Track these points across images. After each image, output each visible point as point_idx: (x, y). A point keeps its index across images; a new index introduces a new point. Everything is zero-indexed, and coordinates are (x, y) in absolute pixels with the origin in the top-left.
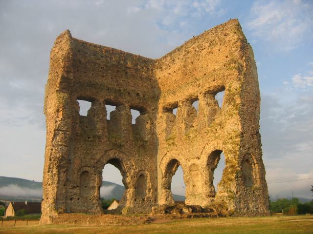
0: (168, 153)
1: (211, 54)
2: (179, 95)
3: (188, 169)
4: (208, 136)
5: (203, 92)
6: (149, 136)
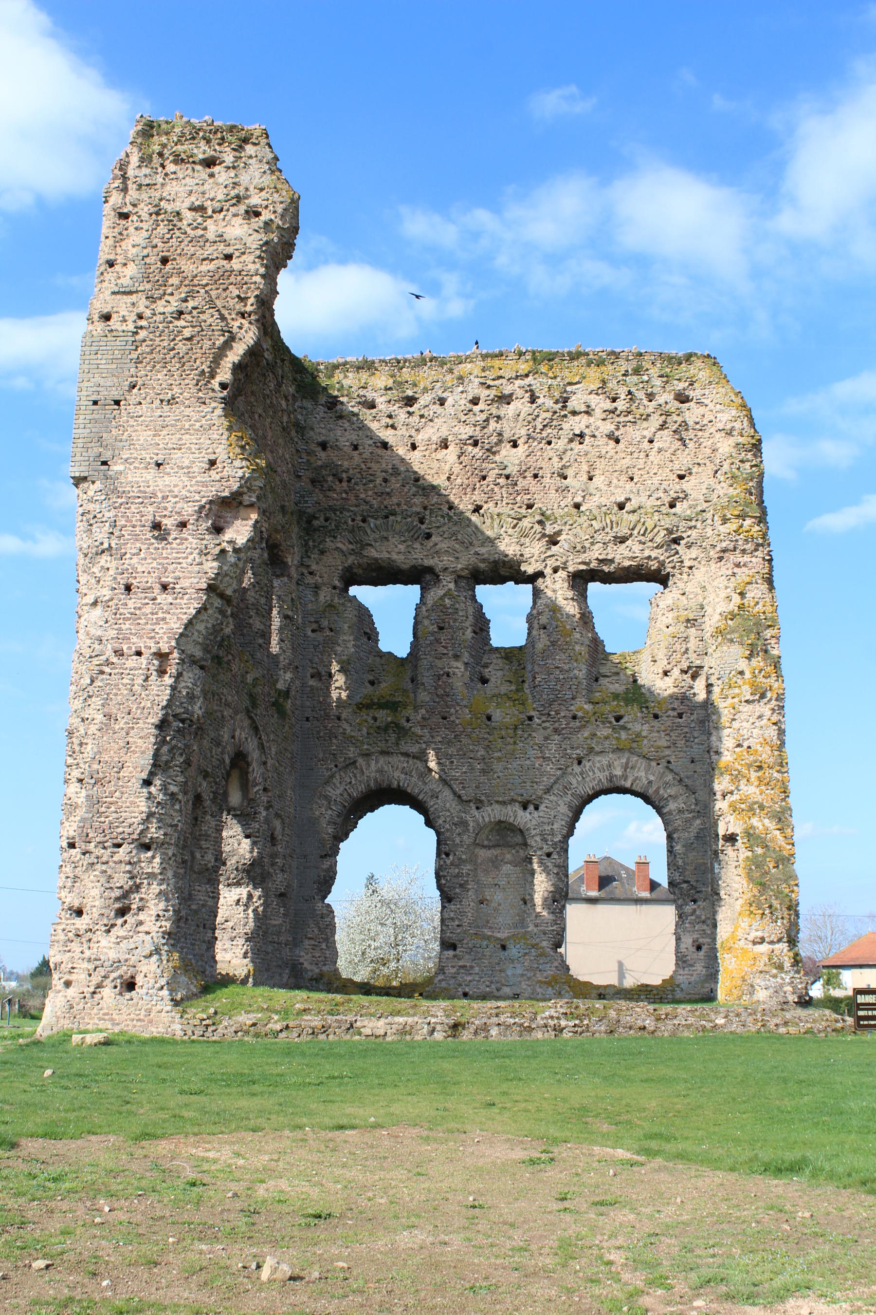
0: (361, 761)
1: (612, 443)
2: (443, 546)
3: (467, 839)
4: (586, 734)
5: (571, 569)
6: (288, 676)
